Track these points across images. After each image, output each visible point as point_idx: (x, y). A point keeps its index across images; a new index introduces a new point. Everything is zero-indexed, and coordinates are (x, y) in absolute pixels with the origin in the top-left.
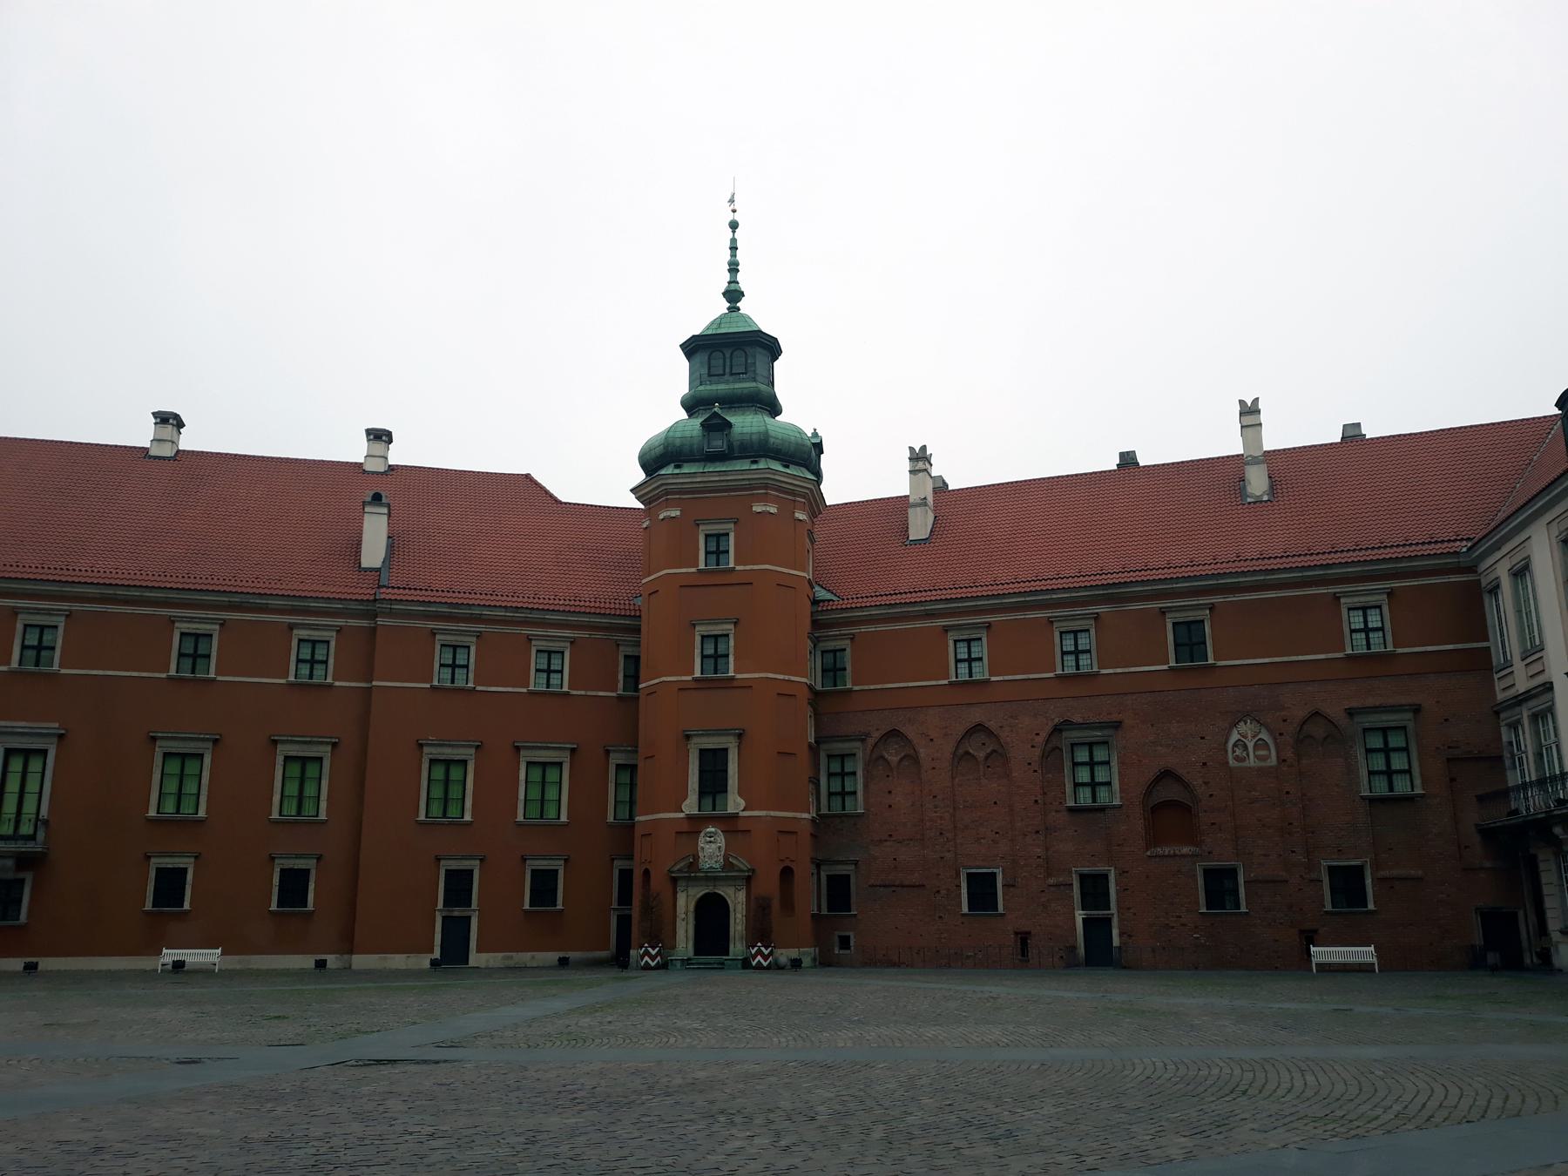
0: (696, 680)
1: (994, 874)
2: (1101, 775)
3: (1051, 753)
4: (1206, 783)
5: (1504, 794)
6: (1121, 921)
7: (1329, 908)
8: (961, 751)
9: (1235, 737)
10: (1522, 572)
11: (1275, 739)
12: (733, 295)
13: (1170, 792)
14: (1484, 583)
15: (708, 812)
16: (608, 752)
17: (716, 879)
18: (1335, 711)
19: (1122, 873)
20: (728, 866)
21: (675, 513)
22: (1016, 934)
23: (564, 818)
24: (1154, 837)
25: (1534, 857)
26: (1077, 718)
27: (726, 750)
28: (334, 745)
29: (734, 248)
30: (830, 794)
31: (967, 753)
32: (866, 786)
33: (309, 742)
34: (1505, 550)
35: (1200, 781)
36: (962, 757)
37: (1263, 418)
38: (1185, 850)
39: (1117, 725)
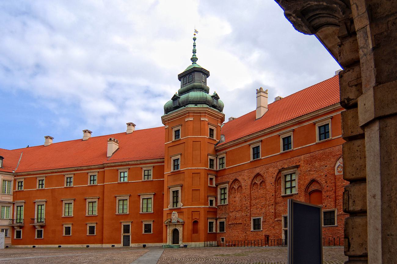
3: (277, 180)
28: (98, 198)
30: (221, 200)
31: (255, 183)
32: (229, 196)
33: (93, 198)
36: (253, 184)
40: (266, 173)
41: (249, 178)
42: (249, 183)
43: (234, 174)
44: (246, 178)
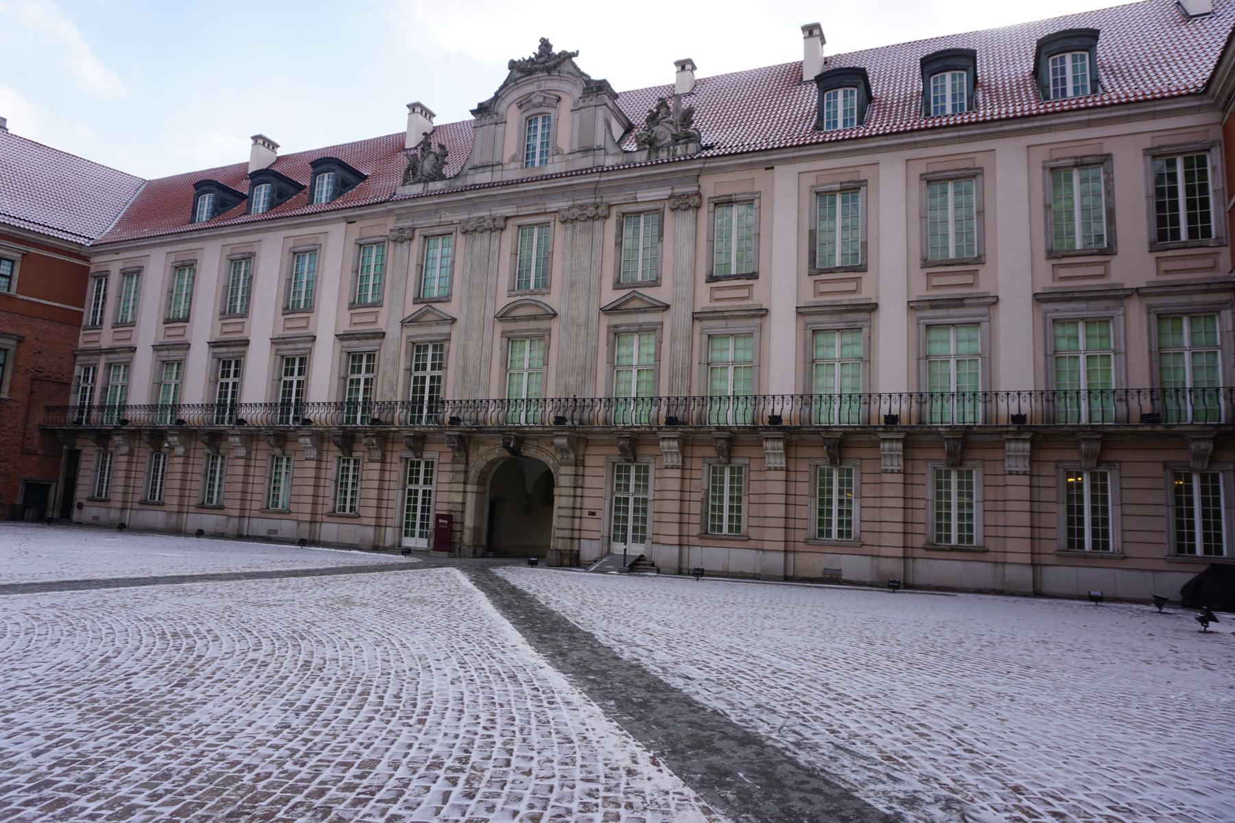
5: (66, 408)
10: (133, 273)
14: (92, 270)
25: (79, 452)
34: (122, 256)
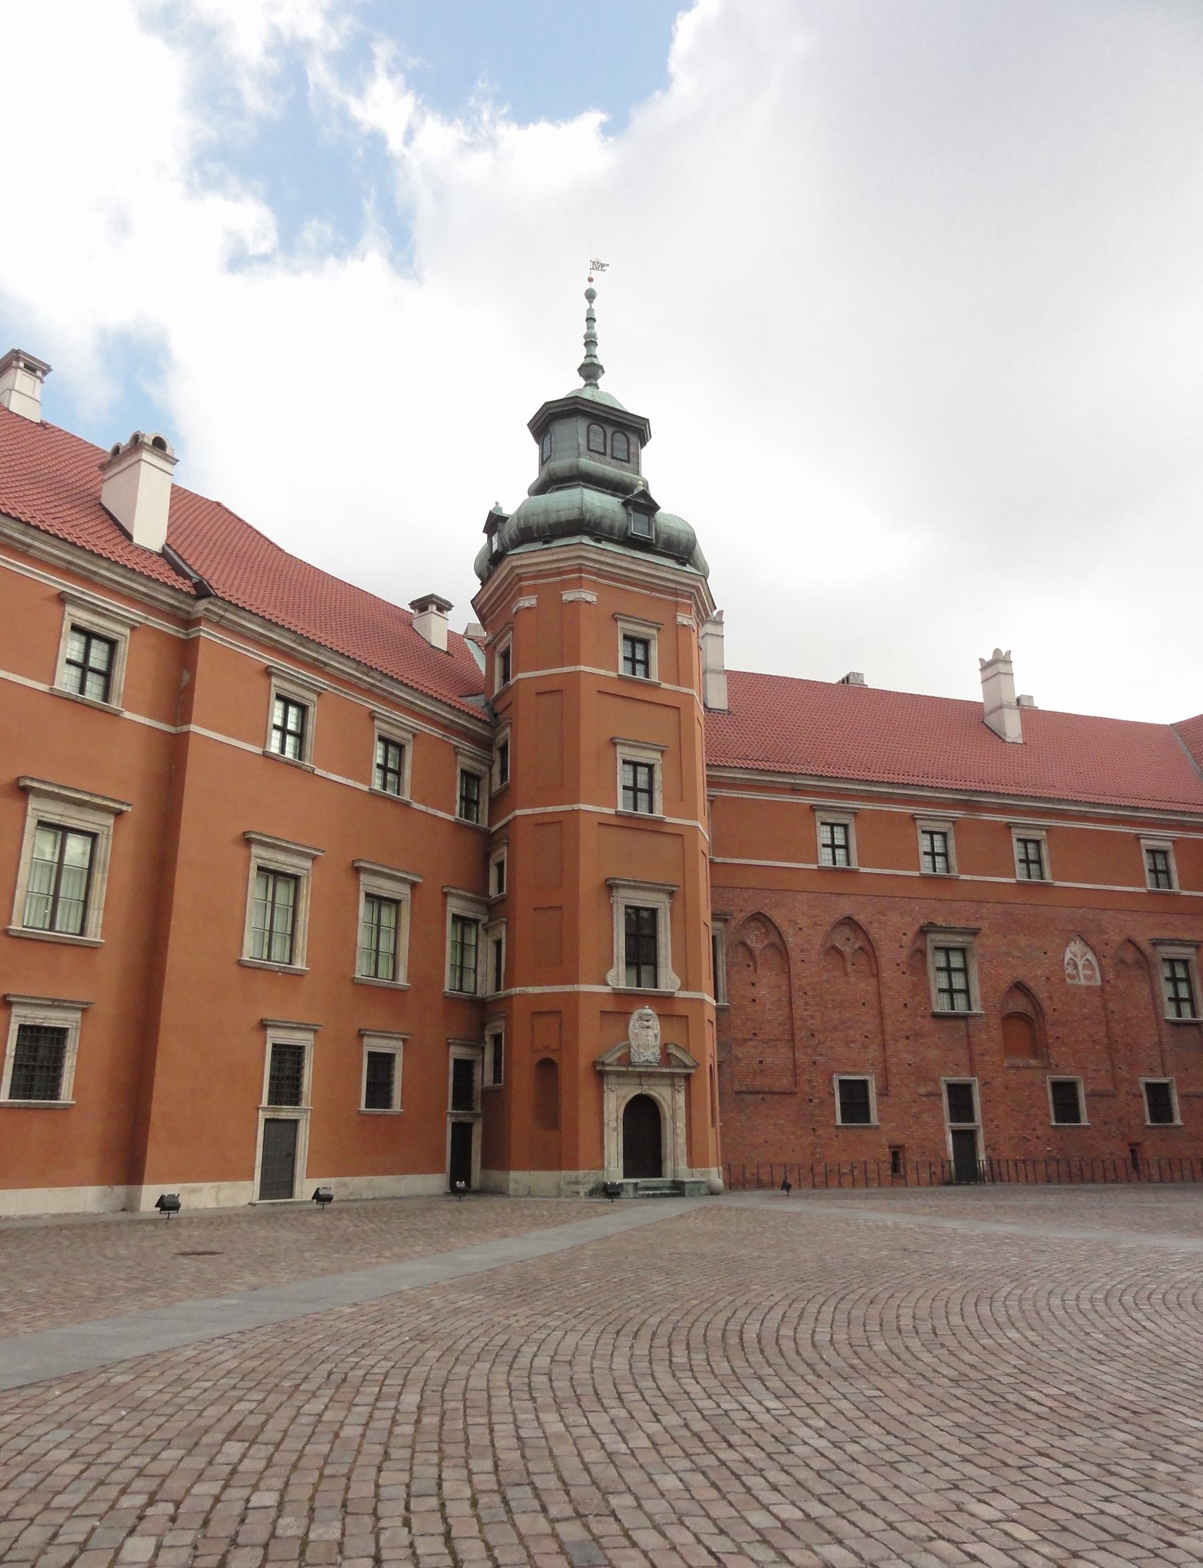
0: (618, 815)
1: (864, 1083)
2: (958, 982)
4: (1051, 998)
6: (986, 1133)
7: (1148, 1123)
8: (829, 945)
9: (1068, 956)
11: (1099, 960)
12: (590, 371)
13: (1020, 1004)
15: (646, 989)
16: (445, 895)
17: (650, 1075)
18: (1143, 941)
19: (985, 1084)
20: (666, 1058)
21: (591, 597)
22: (890, 1147)
23: (402, 981)
24: (1009, 1048)
26: (940, 922)
27: (654, 912)
29: (590, 319)
35: (1045, 995)
37: (1016, 668)
38: (1033, 1062)
39: (975, 932)
40: (875, 925)
41: (815, 924)
42: (817, 942)
43: (750, 892)
44: (802, 922)
